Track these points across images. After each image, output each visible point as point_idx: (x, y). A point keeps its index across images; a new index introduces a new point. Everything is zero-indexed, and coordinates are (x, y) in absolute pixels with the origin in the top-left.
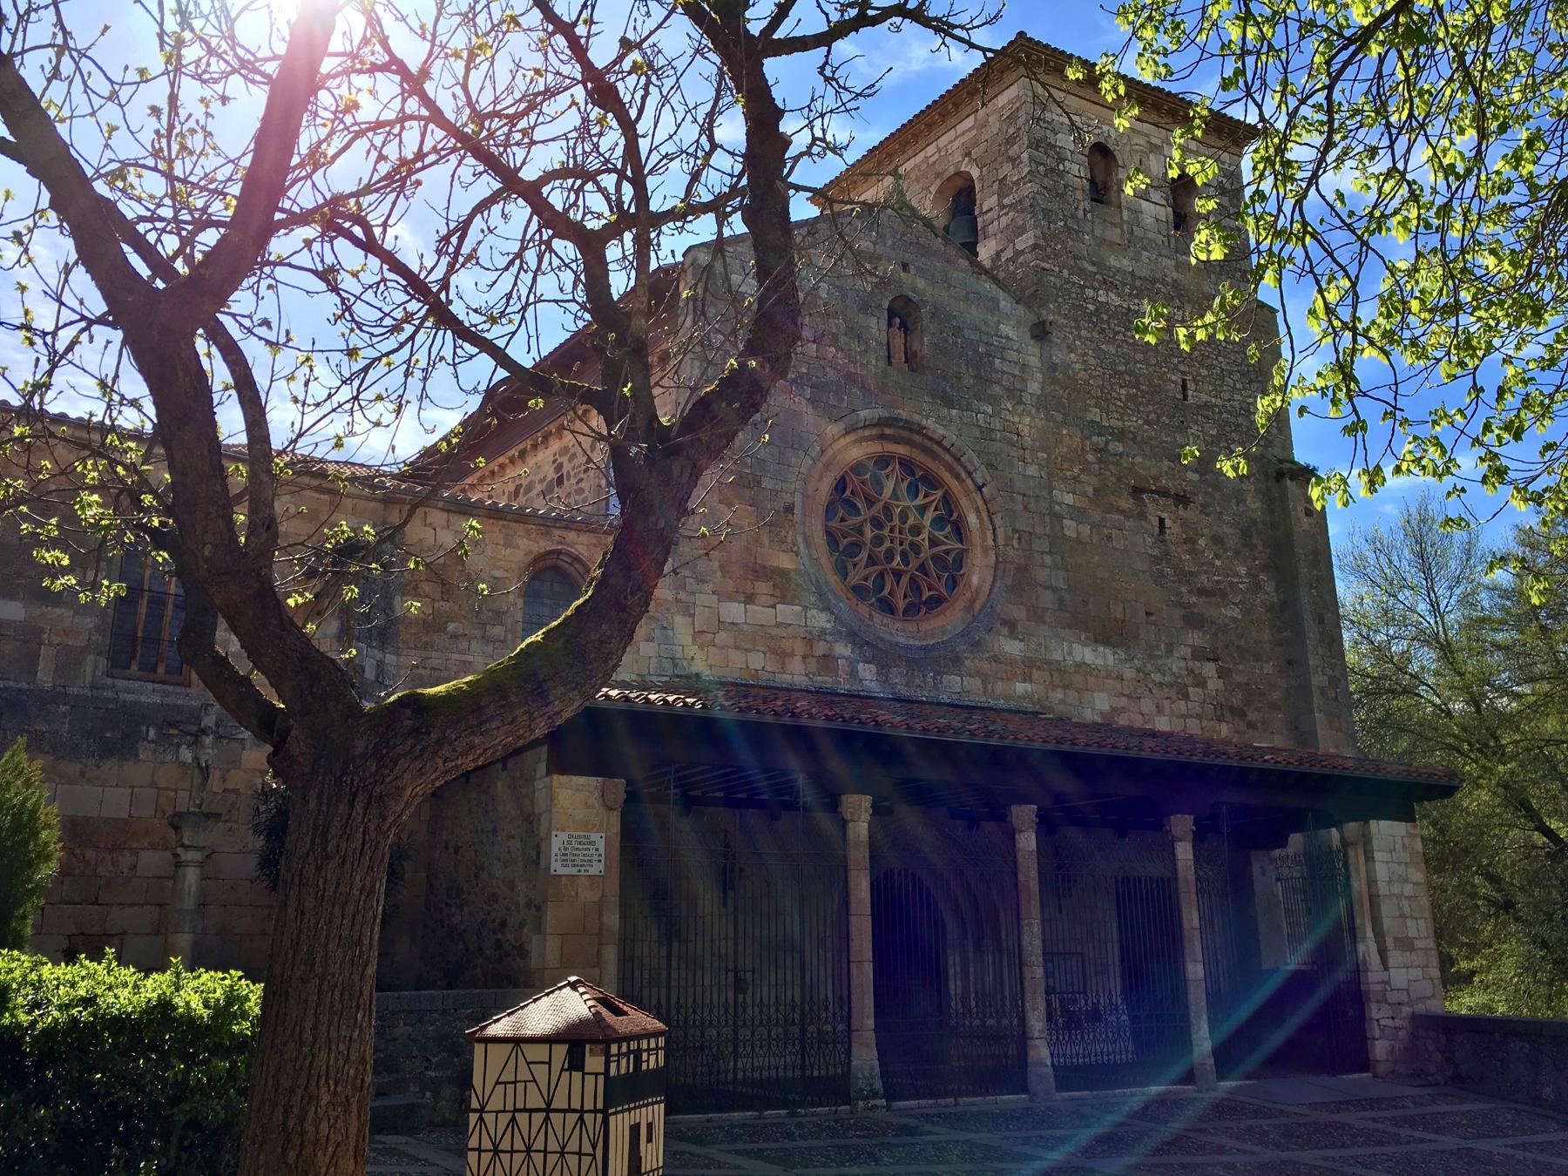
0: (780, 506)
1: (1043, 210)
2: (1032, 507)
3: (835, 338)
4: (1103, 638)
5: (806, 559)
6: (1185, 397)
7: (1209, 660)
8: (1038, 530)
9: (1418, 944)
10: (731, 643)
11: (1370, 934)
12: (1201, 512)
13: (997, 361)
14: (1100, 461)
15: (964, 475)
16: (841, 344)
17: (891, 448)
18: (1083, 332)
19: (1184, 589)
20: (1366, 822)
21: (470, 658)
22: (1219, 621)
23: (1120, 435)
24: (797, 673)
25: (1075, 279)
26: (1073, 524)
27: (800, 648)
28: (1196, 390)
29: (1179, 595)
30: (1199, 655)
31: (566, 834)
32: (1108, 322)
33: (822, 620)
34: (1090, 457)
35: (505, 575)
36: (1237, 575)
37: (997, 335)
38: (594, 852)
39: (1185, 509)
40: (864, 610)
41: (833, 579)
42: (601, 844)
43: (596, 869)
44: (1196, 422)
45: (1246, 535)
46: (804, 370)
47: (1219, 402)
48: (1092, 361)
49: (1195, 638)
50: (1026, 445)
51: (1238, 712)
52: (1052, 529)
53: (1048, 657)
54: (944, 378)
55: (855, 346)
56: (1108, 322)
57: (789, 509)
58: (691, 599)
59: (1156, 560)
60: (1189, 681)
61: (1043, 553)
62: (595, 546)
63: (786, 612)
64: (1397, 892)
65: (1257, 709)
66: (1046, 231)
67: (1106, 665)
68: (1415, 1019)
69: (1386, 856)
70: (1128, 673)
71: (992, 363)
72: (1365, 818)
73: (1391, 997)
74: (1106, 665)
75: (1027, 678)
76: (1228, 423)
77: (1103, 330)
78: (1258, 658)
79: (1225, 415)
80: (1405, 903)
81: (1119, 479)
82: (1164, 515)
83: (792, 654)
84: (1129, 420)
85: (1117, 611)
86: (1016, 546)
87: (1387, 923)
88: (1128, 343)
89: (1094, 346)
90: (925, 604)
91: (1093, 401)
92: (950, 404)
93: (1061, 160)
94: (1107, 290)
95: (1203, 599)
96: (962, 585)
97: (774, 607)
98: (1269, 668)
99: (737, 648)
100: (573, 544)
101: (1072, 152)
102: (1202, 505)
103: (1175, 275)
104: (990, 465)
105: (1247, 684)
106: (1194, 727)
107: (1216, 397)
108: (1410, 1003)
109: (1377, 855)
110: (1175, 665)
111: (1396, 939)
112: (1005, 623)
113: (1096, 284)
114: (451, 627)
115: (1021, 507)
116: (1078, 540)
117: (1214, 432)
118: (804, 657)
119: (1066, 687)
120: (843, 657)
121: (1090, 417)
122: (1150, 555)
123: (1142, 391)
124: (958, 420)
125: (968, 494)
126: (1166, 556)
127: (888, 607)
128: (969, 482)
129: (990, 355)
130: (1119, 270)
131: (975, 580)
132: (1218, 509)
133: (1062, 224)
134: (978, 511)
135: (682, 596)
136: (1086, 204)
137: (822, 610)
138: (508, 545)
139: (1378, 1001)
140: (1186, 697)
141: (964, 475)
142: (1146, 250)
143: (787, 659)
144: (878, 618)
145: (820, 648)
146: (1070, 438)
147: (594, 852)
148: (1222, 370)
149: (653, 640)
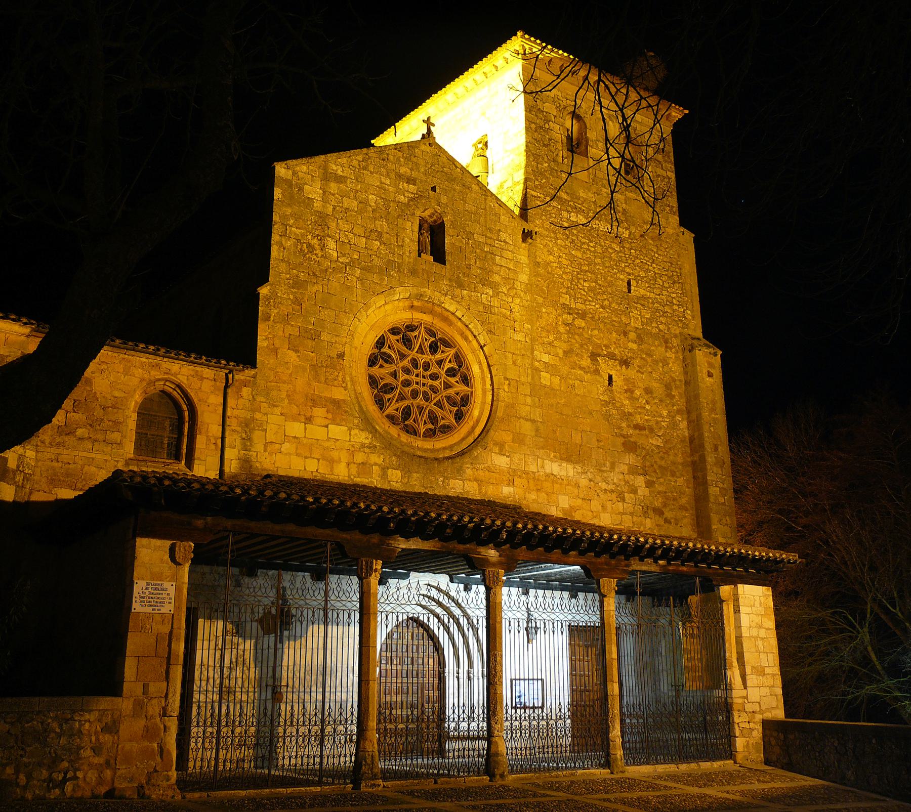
0: (334, 354)
1: (533, 154)
2: (519, 361)
3: (380, 235)
4: (567, 458)
5: (352, 393)
6: (629, 291)
7: (640, 474)
8: (523, 379)
9: (768, 671)
10: (293, 450)
11: (735, 664)
12: (638, 371)
14: (568, 332)
16: (384, 240)
17: (418, 316)
18: (559, 242)
20: (736, 586)
21: (93, 455)
22: (648, 448)
23: (583, 315)
24: (342, 473)
26: (548, 375)
27: (344, 457)
28: (637, 286)
29: (620, 428)
30: (633, 471)
31: (145, 582)
32: (577, 235)
33: (363, 437)
34: (562, 329)
35: (123, 395)
36: (661, 416)
38: (166, 596)
39: (627, 368)
40: (394, 431)
41: (372, 408)
42: (172, 591)
43: (168, 608)
45: (668, 387)
46: (356, 257)
48: (565, 262)
49: (631, 459)
50: (516, 318)
51: (659, 512)
52: (533, 378)
54: (459, 268)
55: (394, 241)
56: (577, 235)
57: (341, 356)
58: (264, 418)
59: (607, 403)
60: (625, 489)
61: (525, 395)
62: (193, 376)
63: (337, 431)
64: (755, 634)
65: (671, 510)
66: (535, 169)
68: (766, 724)
69: (748, 610)
70: (584, 482)
71: (494, 259)
72: (735, 584)
73: (749, 707)
75: (511, 483)
76: (657, 310)
77: (573, 241)
78: (673, 474)
79: (656, 305)
80: (760, 643)
81: (582, 346)
82: (612, 373)
83: (340, 461)
84: (590, 305)
85: (577, 438)
86: (507, 390)
87: (747, 656)
88: (589, 250)
89: (567, 251)
90: (437, 430)
91: (565, 290)
92: (461, 286)
93: (547, 121)
94: (577, 213)
95: (637, 432)
96: (467, 416)
97: (327, 426)
98: (681, 481)
99: (297, 455)
100: (175, 375)
101: (555, 116)
103: (624, 206)
104: (490, 332)
105: (665, 492)
106: (627, 523)
107: (650, 292)
108: (761, 712)
109: (742, 609)
110: (615, 477)
111: (753, 667)
112: (496, 444)
113: (569, 208)
114: (80, 432)
117: (648, 316)
118: (348, 464)
119: (538, 490)
120: (376, 464)
121: (563, 301)
122: (602, 400)
124: (467, 298)
125: (474, 352)
126: (612, 401)
127: (412, 431)
128: (474, 342)
129: (493, 254)
130: (585, 200)
131: (476, 413)
132: (650, 370)
133: (547, 165)
134: (480, 363)
135: (258, 416)
136: (565, 153)
137: (362, 430)
138: (126, 372)
139: (739, 711)
141: (471, 337)
143: (335, 463)
144: (405, 438)
145: (360, 457)
146: (549, 315)
147: (166, 596)
148: (655, 273)
149: (234, 447)
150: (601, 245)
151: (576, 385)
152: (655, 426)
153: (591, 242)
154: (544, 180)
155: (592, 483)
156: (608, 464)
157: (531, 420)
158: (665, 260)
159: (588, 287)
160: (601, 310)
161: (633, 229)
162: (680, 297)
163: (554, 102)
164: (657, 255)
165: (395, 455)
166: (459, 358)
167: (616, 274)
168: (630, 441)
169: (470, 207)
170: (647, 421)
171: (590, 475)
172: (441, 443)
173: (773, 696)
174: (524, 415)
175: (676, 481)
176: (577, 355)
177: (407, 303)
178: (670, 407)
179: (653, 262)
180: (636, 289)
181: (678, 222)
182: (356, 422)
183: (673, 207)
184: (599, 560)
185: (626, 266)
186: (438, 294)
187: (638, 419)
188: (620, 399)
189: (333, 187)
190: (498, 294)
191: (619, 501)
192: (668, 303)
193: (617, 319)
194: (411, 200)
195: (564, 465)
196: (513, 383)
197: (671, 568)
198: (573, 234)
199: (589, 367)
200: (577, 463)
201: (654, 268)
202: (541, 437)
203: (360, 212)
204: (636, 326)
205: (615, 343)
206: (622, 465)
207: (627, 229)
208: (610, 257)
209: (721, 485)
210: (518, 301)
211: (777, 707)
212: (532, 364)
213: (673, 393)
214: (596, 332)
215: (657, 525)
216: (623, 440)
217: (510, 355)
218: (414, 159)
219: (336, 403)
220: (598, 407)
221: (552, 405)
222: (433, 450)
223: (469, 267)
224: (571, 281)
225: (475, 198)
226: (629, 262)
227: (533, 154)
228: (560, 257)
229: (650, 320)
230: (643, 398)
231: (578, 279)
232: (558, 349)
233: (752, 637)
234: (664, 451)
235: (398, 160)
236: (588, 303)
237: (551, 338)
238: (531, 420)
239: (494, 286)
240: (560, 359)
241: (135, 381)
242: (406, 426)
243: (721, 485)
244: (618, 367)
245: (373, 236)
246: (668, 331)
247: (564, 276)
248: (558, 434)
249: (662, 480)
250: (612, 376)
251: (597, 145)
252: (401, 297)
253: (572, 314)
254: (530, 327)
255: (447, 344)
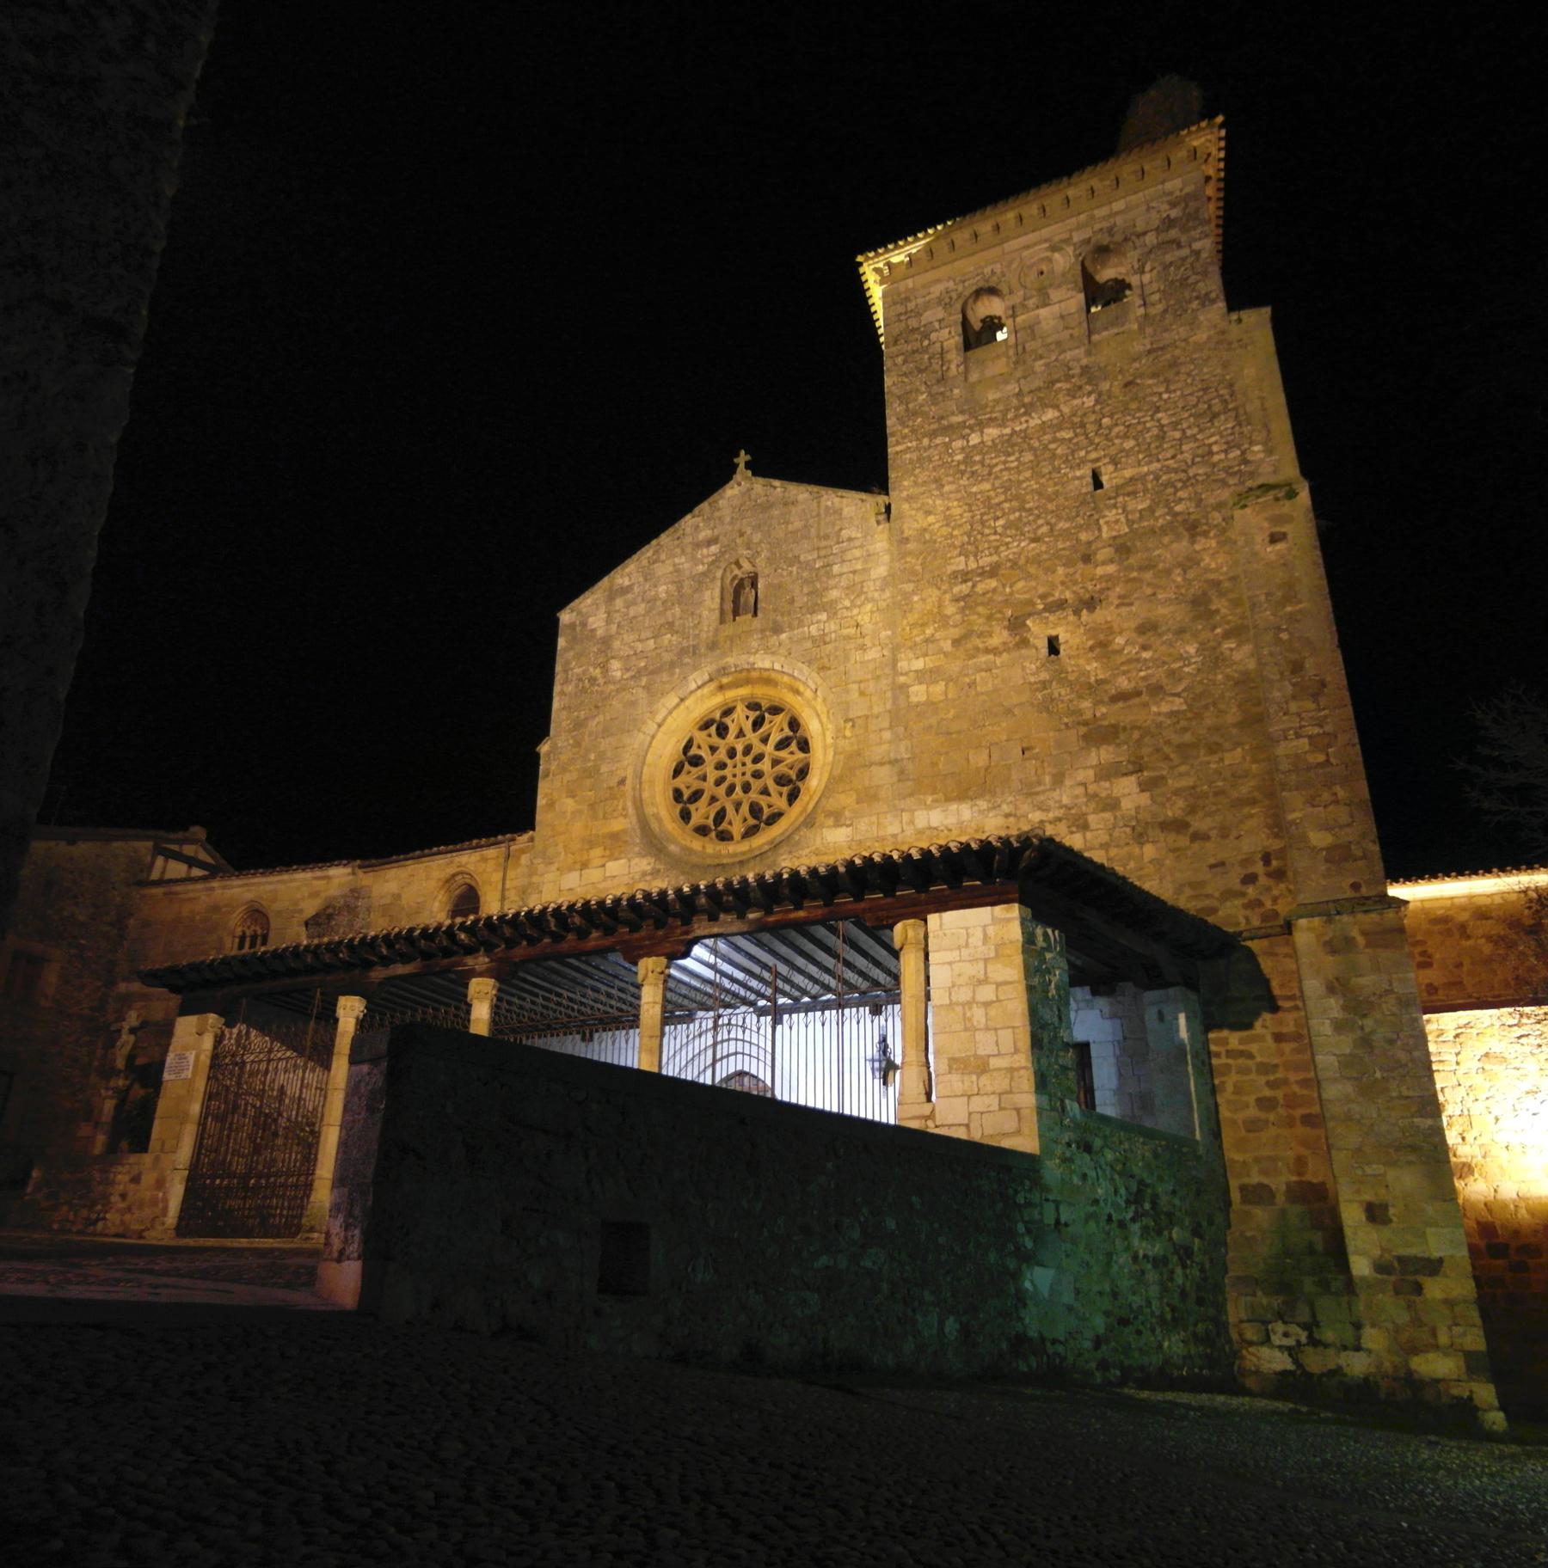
0: (613, 782)
2: (871, 687)
3: (671, 624)
4: (962, 796)
5: (634, 819)
6: (1098, 484)
7: (1126, 774)
9: (994, 1063)
12: (1118, 606)
13: (836, 569)
14: (962, 610)
15: (802, 689)
17: (731, 694)
19: (1086, 704)
23: (993, 572)
25: (938, 440)
26: (923, 688)
28: (1116, 470)
32: (982, 462)
33: (644, 864)
34: (950, 609)
36: (1181, 658)
37: (838, 543)
40: (697, 844)
44: (1115, 506)
46: (643, 664)
47: (1155, 466)
49: (1106, 754)
50: (864, 631)
51: (1178, 826)
52: (894, 703)
53: (881, 833)
54: (775, 610)
57: (622, 782)
59: (1044, 685)
63: (614, 867)
67: (960, 823)
74: (960, 823)
76: (1170, 484)
78: (1213, 749)
79: (1164, 478)
81: (990, 618)
85: (979, 759)
91: (956, 552)
92: (777, 630)
93: (927, 336)
95: (1121, 704)
101: (940, 321)
102: (1120, 597)
105: (1194, 788)
110: (1065, 795)
112: (829, 814)
113: (967, 431)
115: (856, 695)
116: (930, 704)
123: (1031, 509)
125: (808, 703)
126: (1060, 676)
127: (725, 837)
130: (997, 401)
132: (1149, 591)
137: (643, 857)
140: (1085, 827)
142: (1041, 357)
146: (926, 599)
150: (1031, 448)
151: (978, 679)
152: (1164, 681)
153: (1009, 455)
154: (919, 420)
155: (1012, 819)
156: (1047, 779)
157: (890, 762)
158: (1186, 392)
159: (1005, 527)
160: (1033, 545)
161: (1105, 386)
162: (1233, 434)
163: (939, 303)
164: (1165, 396)
165: (683, 873)
166: (794, 724)
167: (1065, 474)
168: (1101, 726)
169: (798, 524)
170: (1144, 679)
171: (1006, 808)
172: (760, 840)
173: (1008, 1112)
174: (877, 758)
175: (1222, 760)
176: (980, 635)
177: (712, 686)
178: (1205, 635)
179: (1158, 410)
180: (1114, 475)
181: (1225, 310)
182: (637, 849)
183: (1207, 294)
184: (636, 935)
185: (1087, 452)
186: (744, 657)
187: (1124, 683)
188: (1078, 666)
189: (619, 603)
190: (835, 613)
191: (1072, 833)
192: (1197, 459)
193: (1068, 543)
194: (713, 563)
195: (954, 807)
196: (859, 722)
197: (771, 919)
198: (975, 463)
199: (1004, 643)
200: (980, 796)
201: (1159, 420)
202: (908, 780)
203: (648, 612)
204: (1114, 533)
205: (1063, 583)
206: (1080, 771)
207: (1089, 394)
208: (1054, 456)
209: (1316, 730)
210: (869, 607)
211: (1018, 1132)
212: (894, 683)
213: (1213, 607)
214: (1020, 585)
215: (1174, 851)
216: (1083, 730)
217: (855, 687)
218: (717, 514)
219: (615, 836)
220: (1025, 697)
221: (931, 727)
222: (751, 850)
223: (792, 601)
224: (969, 535)
225: (803, 510)
226: (1097, 440)
227: (899, 398)
228: (948, 509)
229: (1151, 510)
230: (1133, 644)
231: (983, 523)
232: (942, 643)
233: (957, 1004)
234: (1189, 715)
235: (697, 527)
236: (1002, 548)
237: (929, 631)
238: (890, 762)
239: (831, 609)
240: (946, 654)
241: (432, 884)
242: (722, 832)
243: (1316, 730)
244: (1072, 618)
245: (663, 631)
246: (1198, 506)
247: (955, 533)
248: (941, 766)
249: (1183, 769)
250: (1057, 637)
251: (1024, 306)
252: (700, 683)
253: (970, 580)
254: (889, 633)
255: (775, 710)
